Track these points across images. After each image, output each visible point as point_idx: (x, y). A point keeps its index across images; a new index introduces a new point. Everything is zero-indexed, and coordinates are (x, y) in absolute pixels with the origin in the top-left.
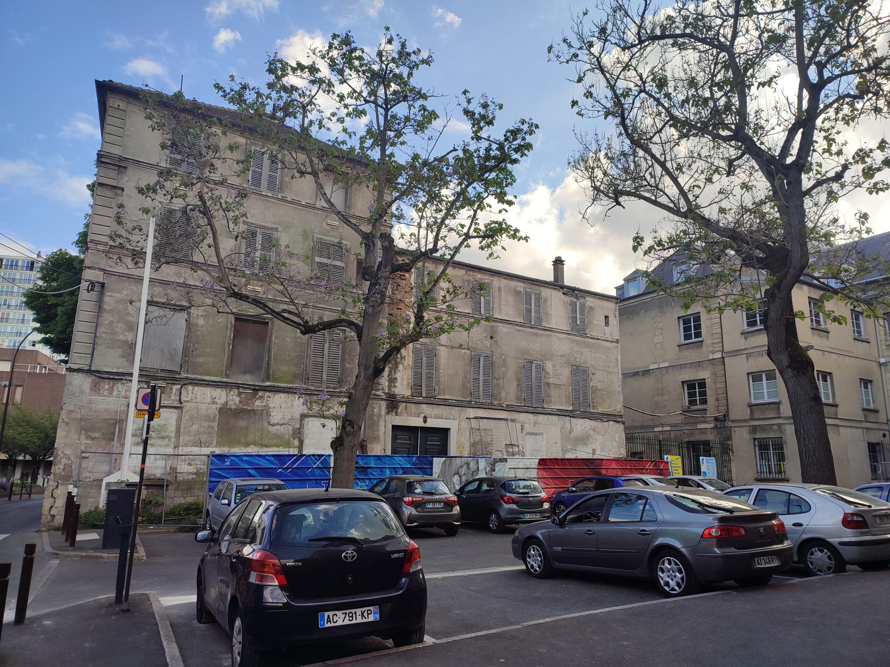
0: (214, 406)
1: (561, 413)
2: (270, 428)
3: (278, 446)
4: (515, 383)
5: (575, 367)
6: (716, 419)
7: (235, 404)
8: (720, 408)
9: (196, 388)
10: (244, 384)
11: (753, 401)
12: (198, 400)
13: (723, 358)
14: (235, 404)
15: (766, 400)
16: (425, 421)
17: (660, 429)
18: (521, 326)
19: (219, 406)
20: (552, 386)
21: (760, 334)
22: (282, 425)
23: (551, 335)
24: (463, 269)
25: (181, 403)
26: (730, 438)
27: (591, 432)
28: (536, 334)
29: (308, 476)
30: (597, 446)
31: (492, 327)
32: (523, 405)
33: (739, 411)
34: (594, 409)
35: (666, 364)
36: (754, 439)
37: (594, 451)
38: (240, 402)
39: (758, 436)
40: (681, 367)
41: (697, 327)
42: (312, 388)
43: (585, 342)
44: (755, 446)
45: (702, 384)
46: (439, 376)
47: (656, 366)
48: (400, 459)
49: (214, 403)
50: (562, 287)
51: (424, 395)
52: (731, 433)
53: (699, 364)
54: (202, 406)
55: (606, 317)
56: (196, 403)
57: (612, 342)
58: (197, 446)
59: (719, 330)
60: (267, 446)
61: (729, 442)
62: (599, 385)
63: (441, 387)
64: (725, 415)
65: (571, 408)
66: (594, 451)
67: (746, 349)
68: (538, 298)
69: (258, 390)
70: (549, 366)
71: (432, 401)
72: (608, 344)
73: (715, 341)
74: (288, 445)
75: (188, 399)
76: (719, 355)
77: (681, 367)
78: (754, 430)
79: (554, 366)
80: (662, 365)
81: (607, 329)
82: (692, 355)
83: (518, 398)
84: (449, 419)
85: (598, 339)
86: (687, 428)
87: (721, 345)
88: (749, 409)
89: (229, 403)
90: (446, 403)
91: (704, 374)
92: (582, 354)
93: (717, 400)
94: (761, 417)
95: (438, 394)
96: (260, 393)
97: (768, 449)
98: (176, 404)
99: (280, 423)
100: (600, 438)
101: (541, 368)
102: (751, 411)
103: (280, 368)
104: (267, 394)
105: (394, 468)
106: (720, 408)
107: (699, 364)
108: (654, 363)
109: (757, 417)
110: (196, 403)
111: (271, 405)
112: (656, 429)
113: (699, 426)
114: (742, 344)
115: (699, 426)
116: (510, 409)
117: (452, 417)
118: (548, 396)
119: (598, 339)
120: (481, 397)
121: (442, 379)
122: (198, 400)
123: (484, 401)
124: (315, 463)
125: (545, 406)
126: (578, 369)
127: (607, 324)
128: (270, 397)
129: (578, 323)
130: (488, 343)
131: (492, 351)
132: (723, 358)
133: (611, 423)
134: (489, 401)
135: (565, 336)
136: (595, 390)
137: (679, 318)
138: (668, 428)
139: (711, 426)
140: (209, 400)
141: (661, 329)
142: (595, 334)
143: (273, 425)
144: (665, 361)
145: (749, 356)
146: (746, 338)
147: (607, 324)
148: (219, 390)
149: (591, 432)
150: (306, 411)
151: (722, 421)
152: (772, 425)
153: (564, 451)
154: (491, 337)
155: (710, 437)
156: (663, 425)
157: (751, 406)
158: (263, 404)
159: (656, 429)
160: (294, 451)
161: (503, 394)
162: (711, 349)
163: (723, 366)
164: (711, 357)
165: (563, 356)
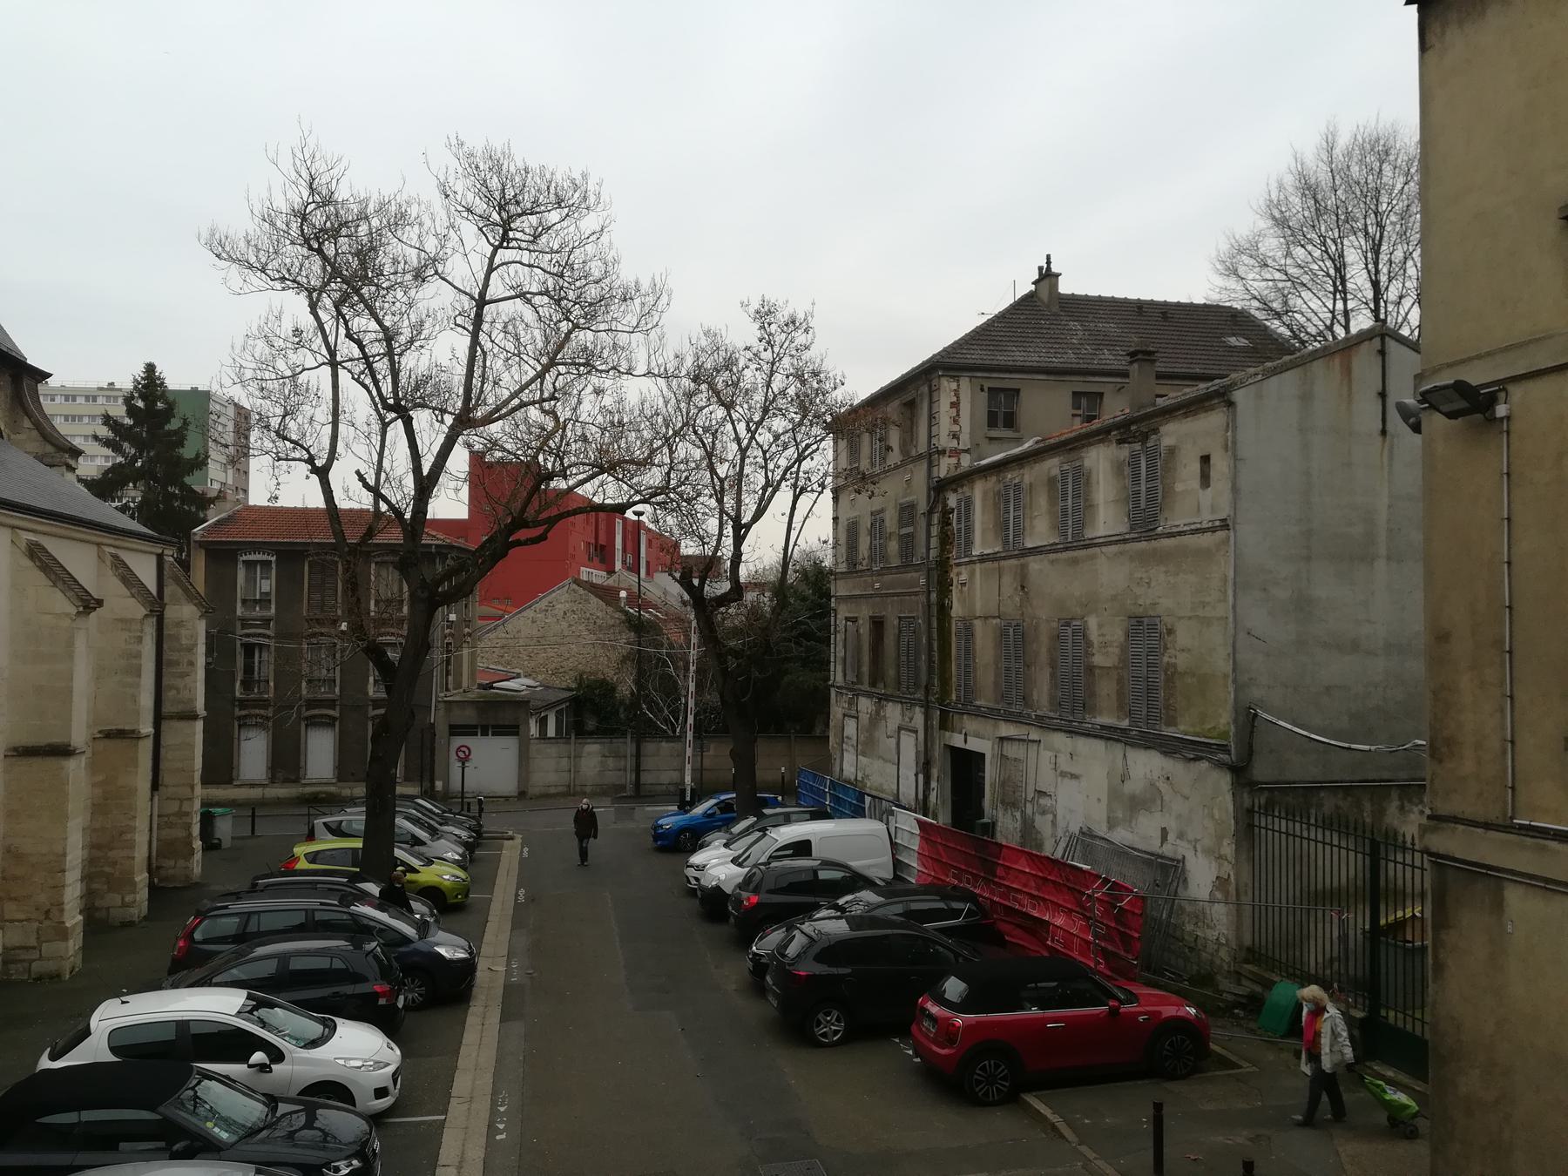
1: (1109, 734)
4: (1047, 672)
5: (1133, 622)
20: (1097, 671)
24: (992, 474)
28: (1075, 561)
30: (1173, 826)
34: (1168, 724)
55: (1205, 459)
57: (1213, 530)
62: (1182, 661)
65: (1125, 723)
70: (1092, 622)
72: (1206, 540)
79: (1100, 626)
81: (1206, 496)
85: (1180, 533)
101: (1082, 633)
116: (1043, 724)
118: (1092, 695)
119: (1180, 533)
126: (1140, 623)
127: (1205, 480)
133: (1204, 765)
136: (1172, 674)
147: (1205, 480)
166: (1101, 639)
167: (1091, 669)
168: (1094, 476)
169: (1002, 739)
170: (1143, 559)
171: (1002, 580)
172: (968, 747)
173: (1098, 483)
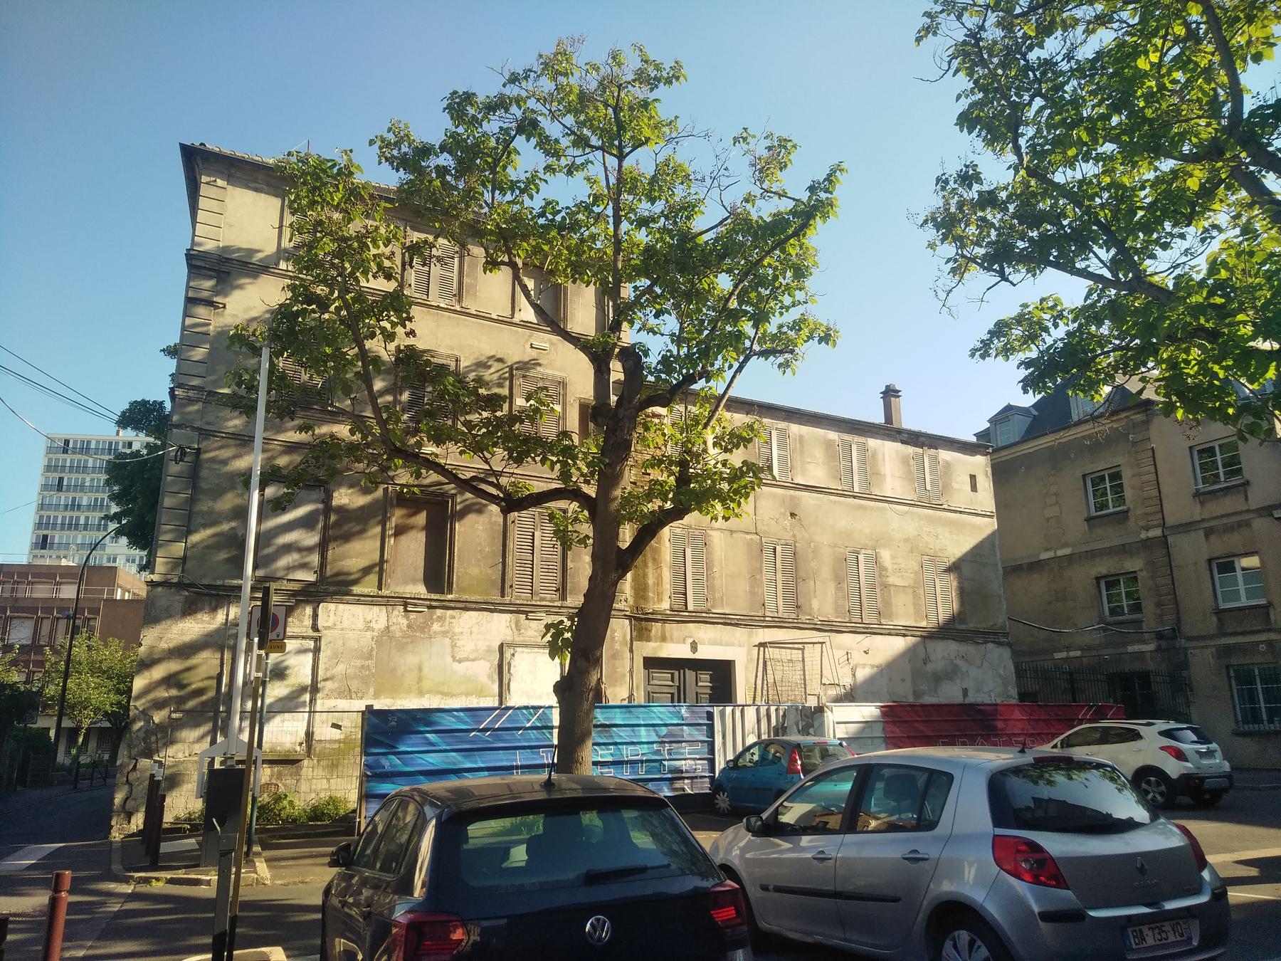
0: (369, 635)
2: (456, 666)
3: (467, 694)
4: (831, 586)
6: (1160, 636)
7: (401, 630)
8: (1166, 618)
9: (341, 606)
10: (414, 599)
11: (1223, 606)
12: (345, 624)
13: (1165, 537)
14: (401, 630)
15: (1244, 602)
16: (694, 647)
17: (1063, 655)
18: (837, 495)
19: (375, 634)
20: (892, 589)
21: (1225, 495)
22: (473, 660)
23: (885, 509)
25: (318, 630)
26: (1185, 665)
27: (961, 663)
29: (519, 741)
30: (968, 684)
31: (792, 498)
32: (847, 620)
33: (1198, 619)
35: (1067, 551)
36: (1227, 667)
37: (965, 692)
38: (409, 626)
39: (1234, 661)
40: (1092, 555)
41: (1118, 489)
42: (518, 602)
43: (940, 518)
44: (1229, 677)
45: (1133, 578)
46: (714, 578)
47: (1050, 554)
48: (662, 709)
49: (369, 629)
50: (900, 432)
51: (690, 608)
52: (1186, 655)
53: (1123, 550)
54: (351, 635)
55: (973, 478)
56: (342, 629)
58: (345, 697)
59: (1155, 493)
60: (451, 695)
61: (1185, 673)
63: (717, 596)
64: (1174, 630)
66: (965, 692)
67: (1203, 520)
68: (864, 449)
69: (435, 607)
70: (886, 556)
71: (702, 618)
73: (1150, 510)
74: (481, 693)
75: (329, 624)
76: (1157, 532)
77: (1092, 555)
78: (1226, 652)
79: (893, 557)
80: (1060, 553)
82: (1111, 537)
83: (837, 609)
84: (732, 645)
85: (961, 512)
86: (1110, 651)
87: (1160, 516)
88: (1214, 619)
89: (391, 628)
90: (728, 621)
91: (1134, 564)
92: (937, 537)
93: (1159, 605)
94: (1239, 630)
95: (713, 607)
96: (439, 612)
97: (1253, 682)
98: (311, 633)
99: (472, 657)
100: (974, 672)
102: (1219, 620)
103: (469, 571)
104: (449, 612)
105: (653, 725)
106: (1166, 618)
107: (1123, 550)
108: (1047, 550)
109: (1230, 630)
110: (342, 629)
111: (457, 630)
112: (1057, 656)
113: (1130, 649)
114: (1196, 512)
115: (1130, 649)
117: (736, 642)
119: (961, 512)
120: (781, 608)
121: (717, 583)
122: (345, 624)
123: (786, 615)
124: (529, 720)
125: (883, 621)
127: (974, 488)
128: (453, 617)
129: (928, 487)
130: (788, 521)
131: (794, 536)
132: (1165, 537)
133: (990, 646)
134: (794, 616)
135: (906, 508)
137: (1084, 476)
138: (1078, 653)
139: (1151, 647)
140: (360, 625)
141: (1056, 495)
142: (954, 506)
143: (460, 661)
144: (1066, 545)
145: (1209, 533)
146: (1202, 503)
147: (974, 488)
148: (376, 609)
149: (961, 663)
150: (509, 639)
151: (1169, 638)
152: (1258, 643)
153: (916, 694)
154: (793, 515)
155: (1151, 665)
156: (1068, 648)
157: (1219, 613)
158: (443, 629)
159: (1057, 656)
160: (492, 702)
161: (815, 604)
162: (1142, 523)
163: (1165, 551)
164: (1143, 535)
165: (906, 540)
166: (895, 566)
167: (886, 586)
168: (880, 457)
169: (762, 645)
170: (930, 520)
171: (758, 502)
172: (699, 656)
173: (884, 459)
